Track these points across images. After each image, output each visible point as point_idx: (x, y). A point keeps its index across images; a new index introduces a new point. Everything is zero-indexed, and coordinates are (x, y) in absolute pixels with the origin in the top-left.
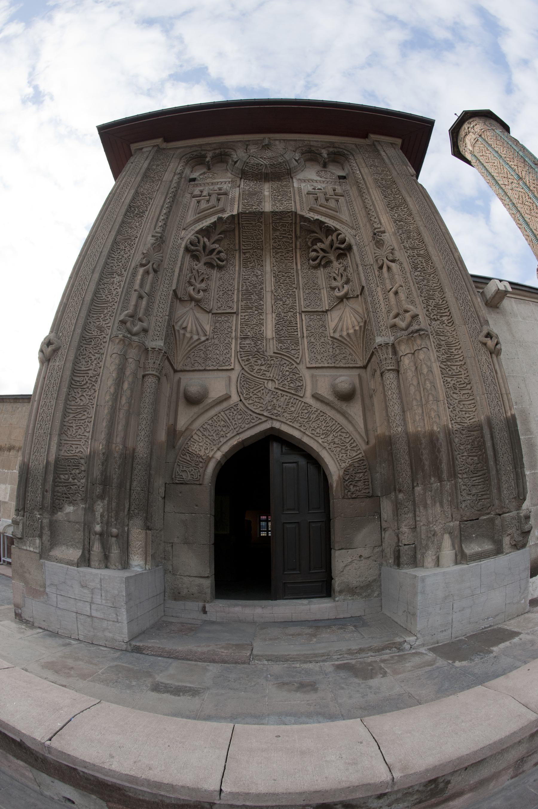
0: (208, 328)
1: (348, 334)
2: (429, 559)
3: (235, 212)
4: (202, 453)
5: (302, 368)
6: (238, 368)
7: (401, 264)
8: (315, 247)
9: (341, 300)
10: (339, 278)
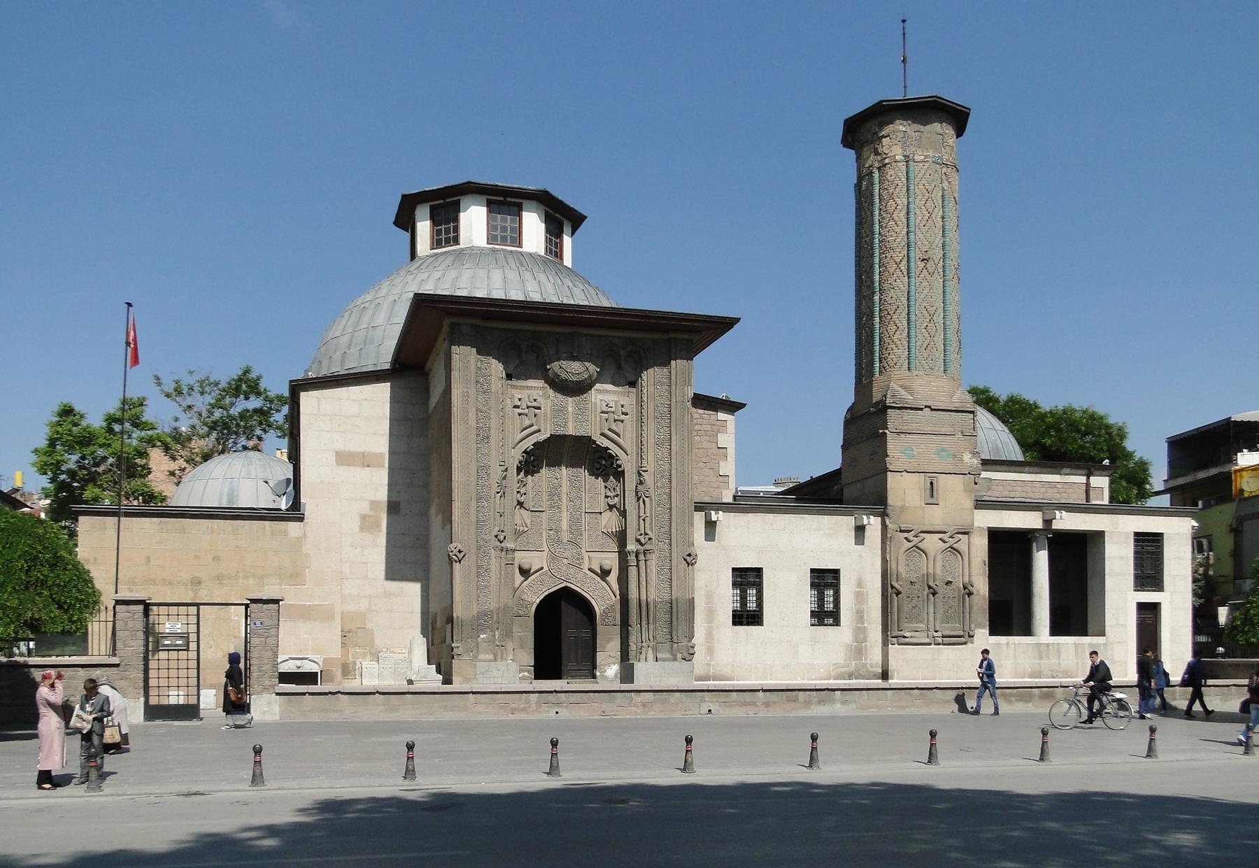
1: (612, 532)
3: (549, 436)
4: (529, 600)
5: (583, 550)
7: (651, 500)
8: (600, 461)
9: (611, 507)
10: (612, 490)
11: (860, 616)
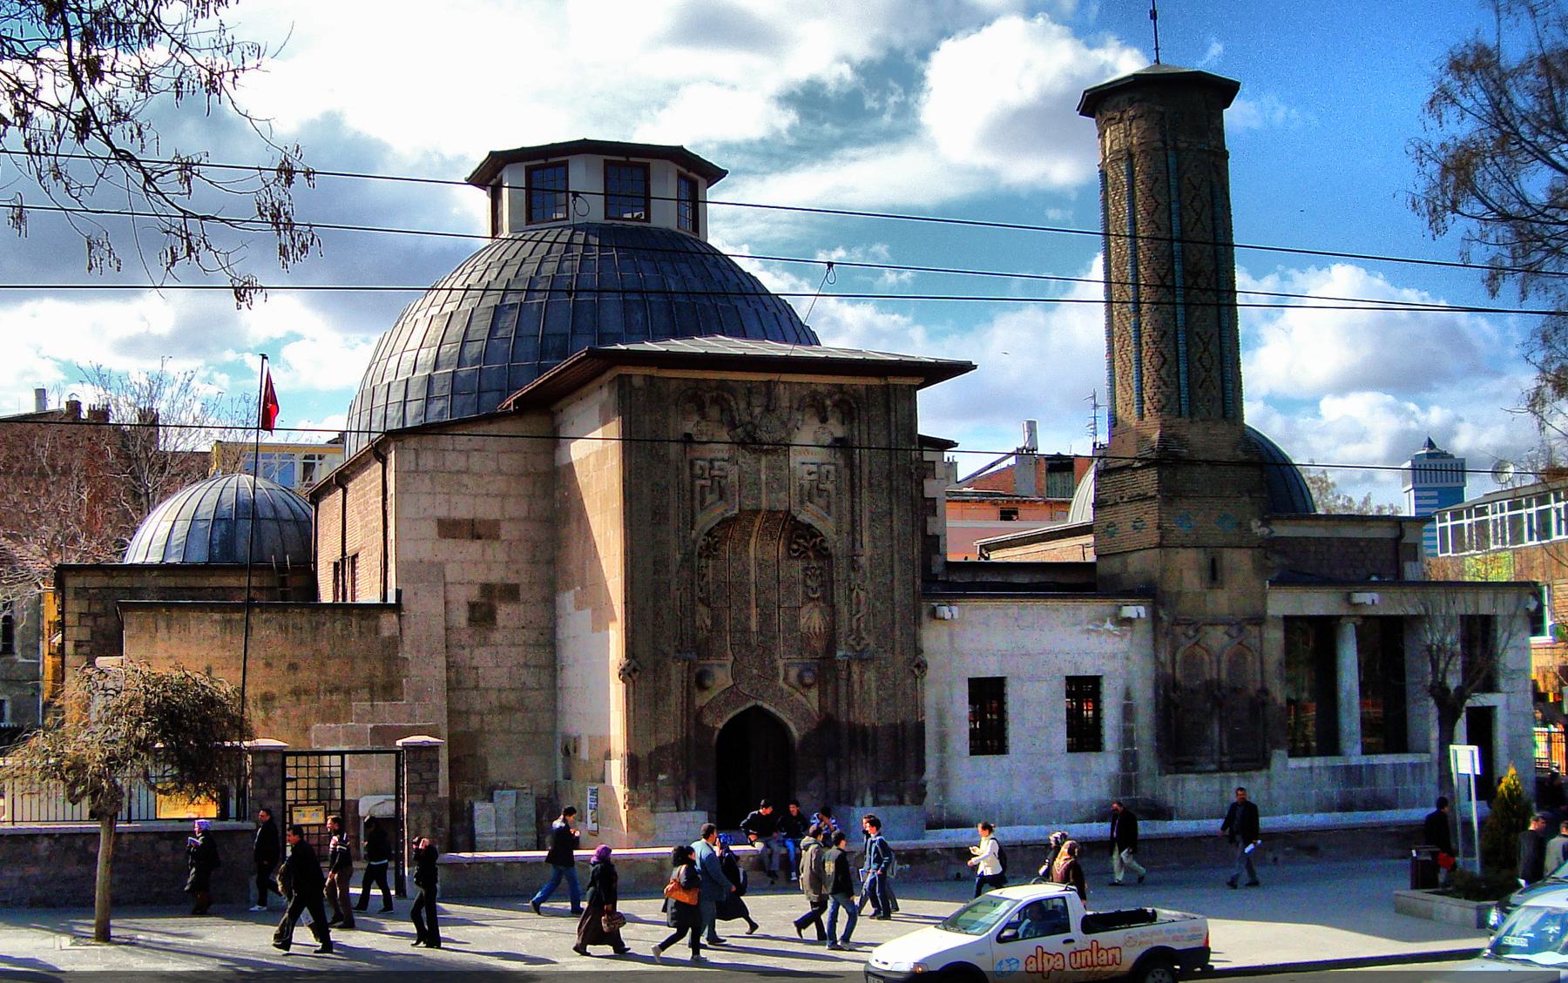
0: (709, 622)
2: (858, 803)
6: (732, 658)
11: (1127, 737)
